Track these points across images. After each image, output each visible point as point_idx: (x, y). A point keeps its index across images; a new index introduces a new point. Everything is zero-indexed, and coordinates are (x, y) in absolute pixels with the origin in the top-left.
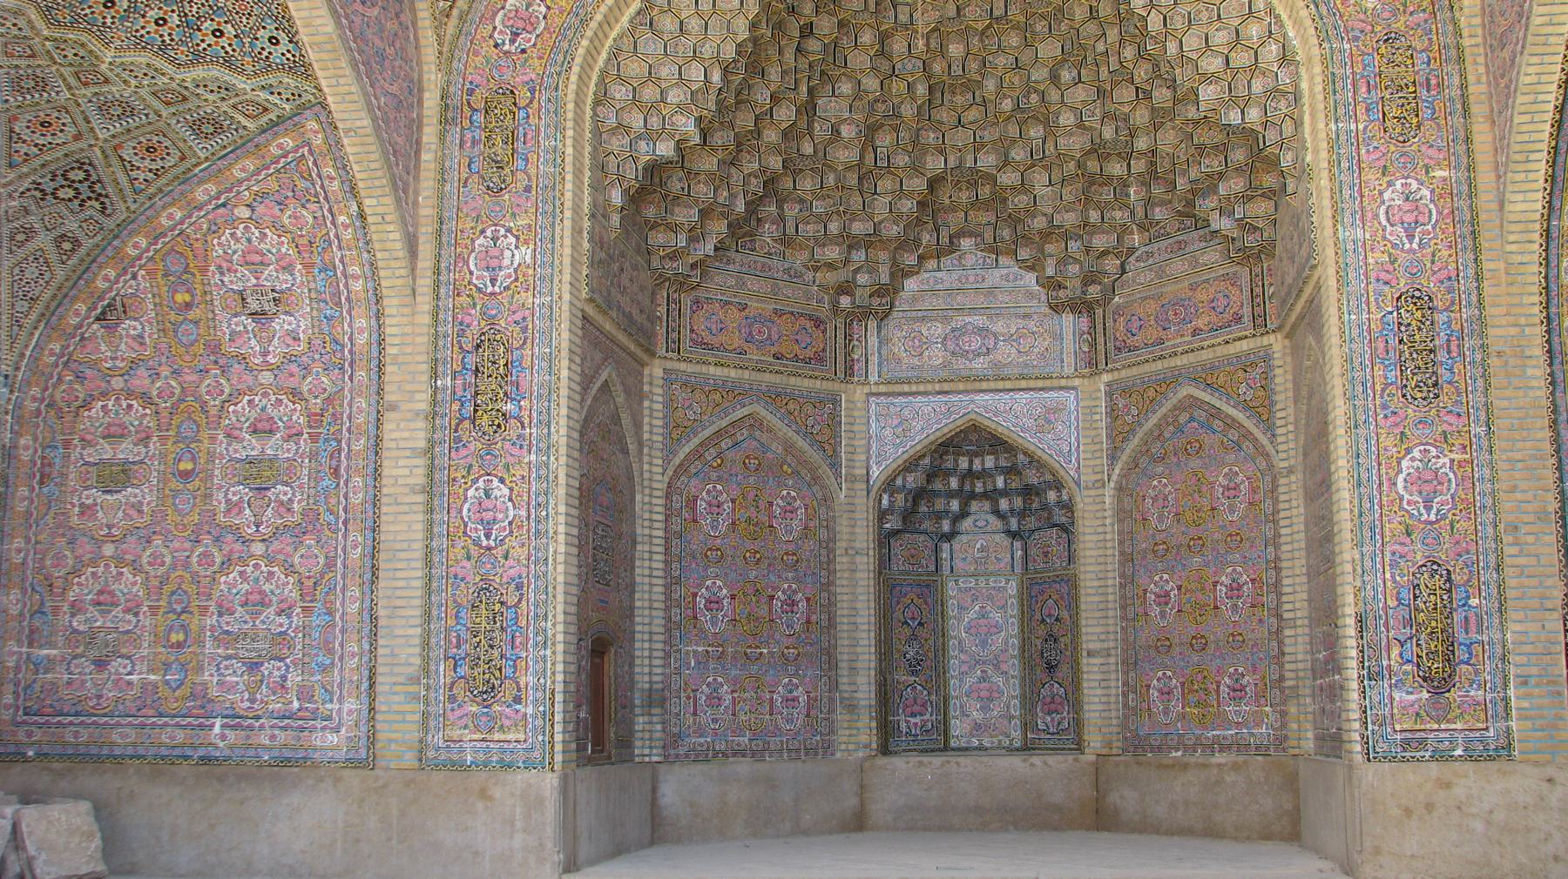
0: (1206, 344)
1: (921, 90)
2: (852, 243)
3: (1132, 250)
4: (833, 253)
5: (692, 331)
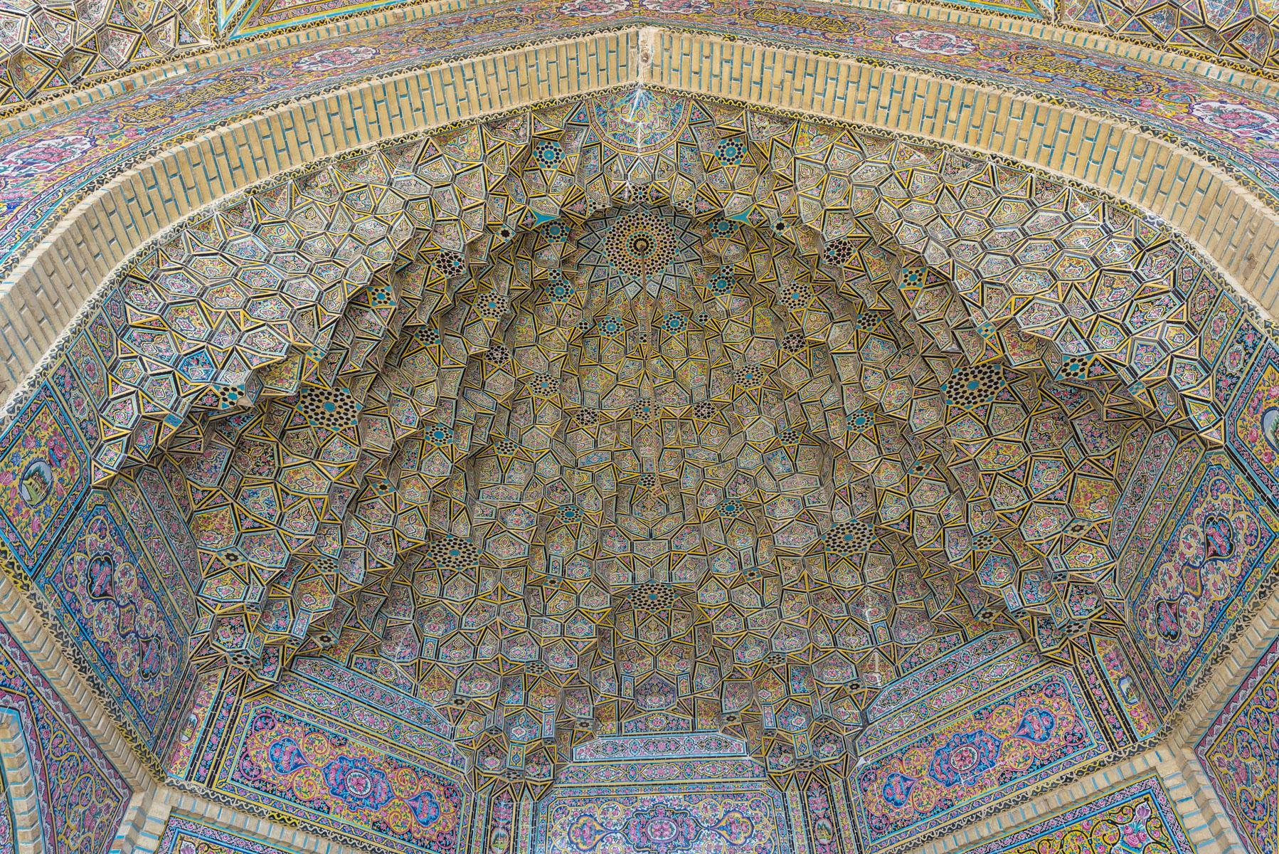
1: (607, 485)
4: (481, 690)
5: (245, 756)
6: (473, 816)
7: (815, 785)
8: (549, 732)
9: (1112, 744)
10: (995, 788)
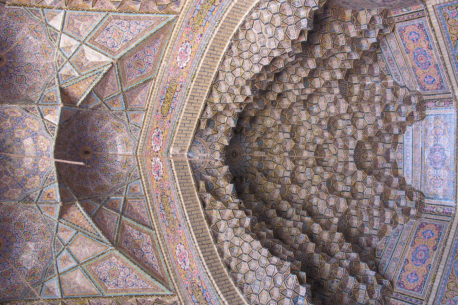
0: (435, 42)
1: (319, 169)
2: (385, 204)
3: (395, 83)
4: (388, 215)
6: (430, 219)
7: (424, 105)
8: (403, 193)
9: (423, 17)
10: (433, 51)
